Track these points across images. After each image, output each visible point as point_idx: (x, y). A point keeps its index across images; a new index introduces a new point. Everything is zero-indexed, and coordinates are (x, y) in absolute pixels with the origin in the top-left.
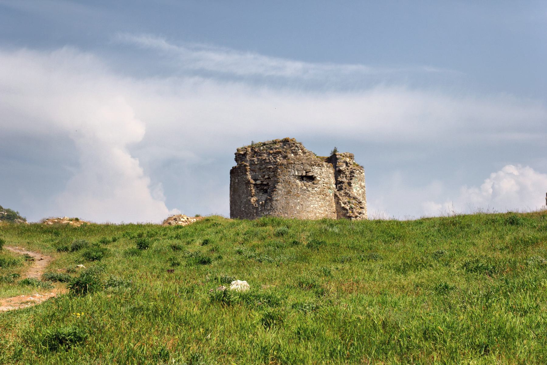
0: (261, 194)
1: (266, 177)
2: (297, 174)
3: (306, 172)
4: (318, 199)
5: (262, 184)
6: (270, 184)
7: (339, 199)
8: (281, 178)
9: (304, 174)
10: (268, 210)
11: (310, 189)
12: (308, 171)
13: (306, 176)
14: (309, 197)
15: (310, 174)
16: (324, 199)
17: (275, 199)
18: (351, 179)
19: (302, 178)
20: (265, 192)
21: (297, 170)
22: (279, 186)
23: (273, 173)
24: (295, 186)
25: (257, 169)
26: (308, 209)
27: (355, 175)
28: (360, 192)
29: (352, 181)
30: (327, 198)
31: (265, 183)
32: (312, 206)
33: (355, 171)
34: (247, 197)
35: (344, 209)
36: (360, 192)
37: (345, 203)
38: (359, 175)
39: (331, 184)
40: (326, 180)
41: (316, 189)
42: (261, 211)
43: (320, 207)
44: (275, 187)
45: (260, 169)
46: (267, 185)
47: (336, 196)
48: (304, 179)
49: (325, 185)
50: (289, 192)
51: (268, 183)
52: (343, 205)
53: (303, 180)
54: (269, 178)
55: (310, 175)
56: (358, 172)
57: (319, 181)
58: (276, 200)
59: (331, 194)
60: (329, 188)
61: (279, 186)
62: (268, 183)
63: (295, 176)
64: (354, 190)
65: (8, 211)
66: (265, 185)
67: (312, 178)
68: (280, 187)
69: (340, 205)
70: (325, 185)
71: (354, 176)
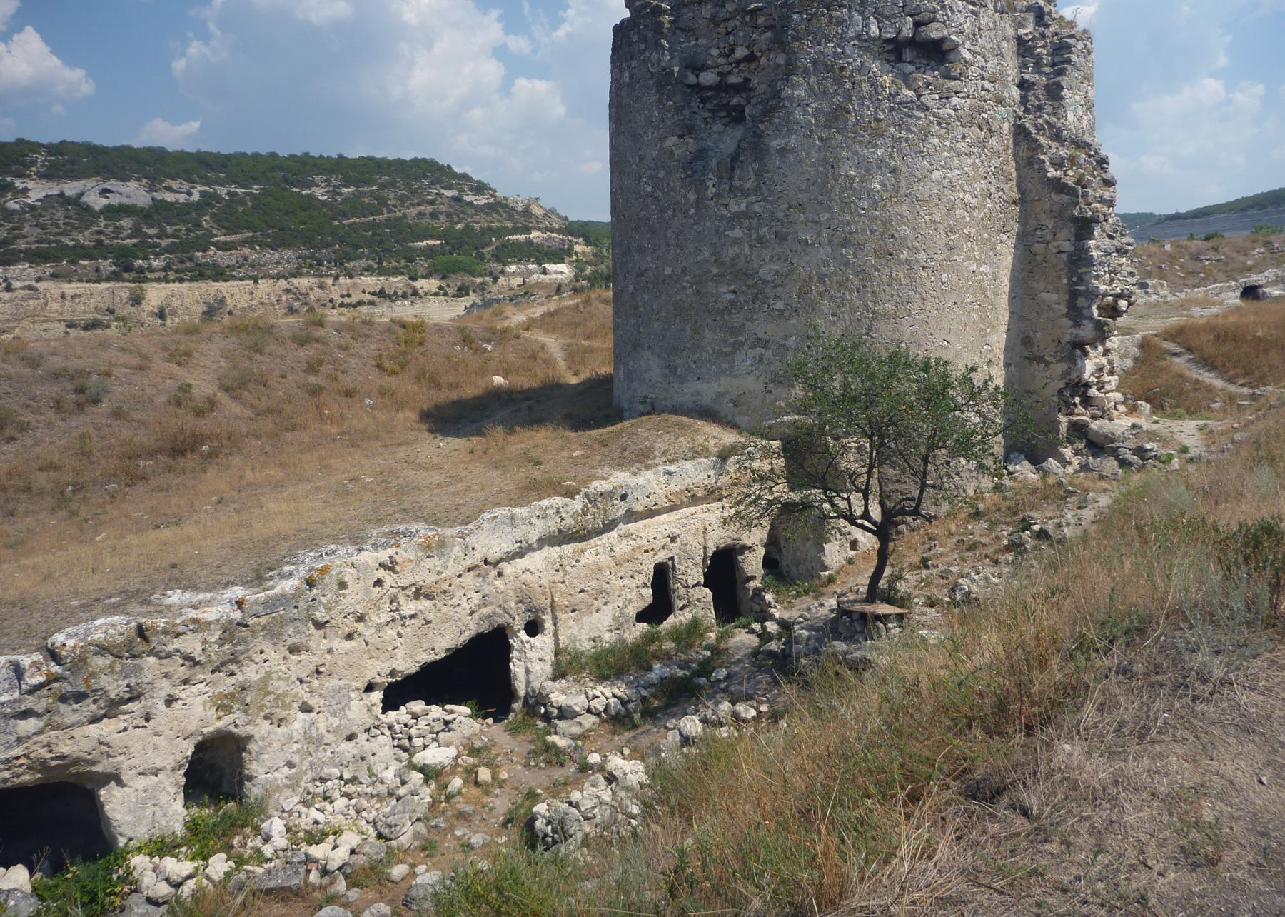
0: (718, 127)
1: (740, 52)
2: (874, 29)
3: (917, 25)
4: (962, 146)
5: (722, 87)
6: (755, 81)
7: (1036, 147)
8: (807, 51)
9: (907, 32)
10: (746, 194)
11: (931, 100)
12: (925, 16)
13: (912, 43)
14: (925, 135)
15: (934, 32)
16: (982, 144)
17: (775, 144)
18: (1061, 73)
19: (894, 51)
20: (737, 116)
21: (878, 14)
22: (798, 90)
23: (768, 35)
24: (866, 87)
25: (703, 23)
26: (921, 191)
27: (1074, 58)
28: (1085, 122)
29: (1064, 81)
30: (993, 141)
31: (734, 80)
32: (937, 175)
33: (1072, 41)
34: (663, 139)
35: (1058, 186)
36: (1085, 122)
37: (1058, 164)
38: (1082, 60)
39: (1005, 85)
40: (992, 65)
41: (955, 100)
42: (718, 195)
43: (971, 179)
44: (777, 95)
45: (714, 21)
46: (744, 87)
47: (1020, 132)
48: (908, 54)
49: (987, 84)
50: (836, 117)
51: (747, 80)
52: (1052, 172)
53: (900, 59)
54: (751, 58)
55: (935, 35)
56: (1080, 46)
57: (967, 64)
58: (783, 151)
59: (1006, 126)
60: (1000, 101)
61: (793, 87)
62: (747, 80)
63: (864, 41)
64: (1070, 117)
65: (478, 182)
66: (737, 89)
67: (937, 53)
68: (800, 93)
69: (1043, 170)
70: (987, 84)
71: (1069, 61)
